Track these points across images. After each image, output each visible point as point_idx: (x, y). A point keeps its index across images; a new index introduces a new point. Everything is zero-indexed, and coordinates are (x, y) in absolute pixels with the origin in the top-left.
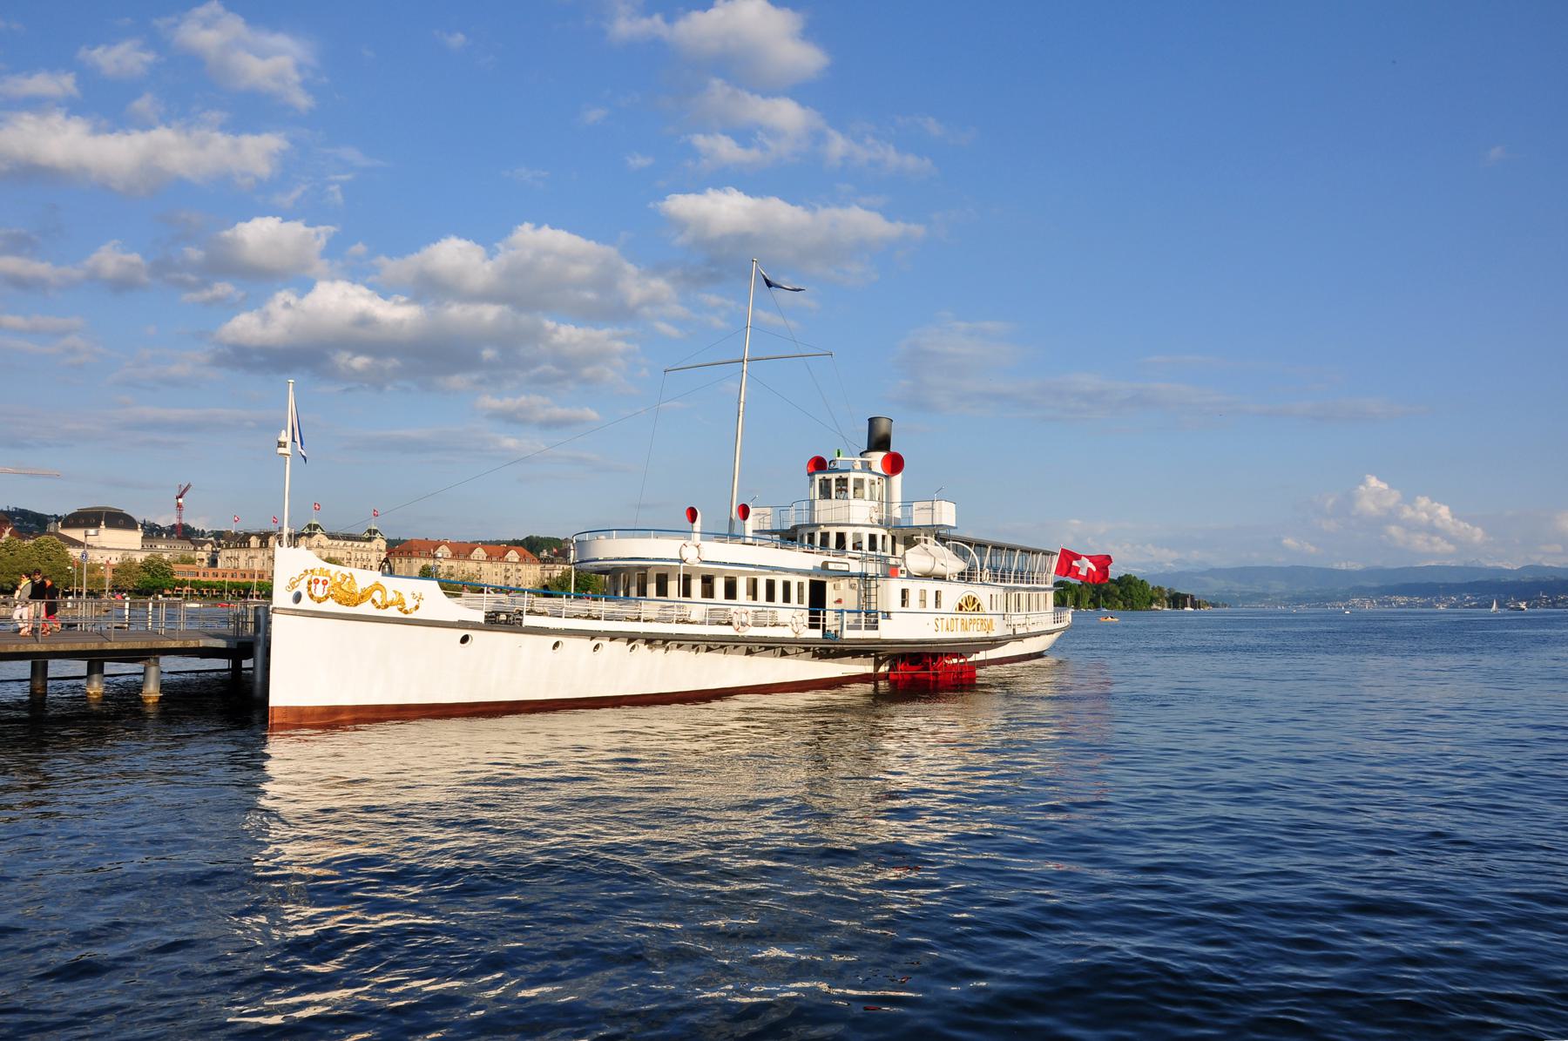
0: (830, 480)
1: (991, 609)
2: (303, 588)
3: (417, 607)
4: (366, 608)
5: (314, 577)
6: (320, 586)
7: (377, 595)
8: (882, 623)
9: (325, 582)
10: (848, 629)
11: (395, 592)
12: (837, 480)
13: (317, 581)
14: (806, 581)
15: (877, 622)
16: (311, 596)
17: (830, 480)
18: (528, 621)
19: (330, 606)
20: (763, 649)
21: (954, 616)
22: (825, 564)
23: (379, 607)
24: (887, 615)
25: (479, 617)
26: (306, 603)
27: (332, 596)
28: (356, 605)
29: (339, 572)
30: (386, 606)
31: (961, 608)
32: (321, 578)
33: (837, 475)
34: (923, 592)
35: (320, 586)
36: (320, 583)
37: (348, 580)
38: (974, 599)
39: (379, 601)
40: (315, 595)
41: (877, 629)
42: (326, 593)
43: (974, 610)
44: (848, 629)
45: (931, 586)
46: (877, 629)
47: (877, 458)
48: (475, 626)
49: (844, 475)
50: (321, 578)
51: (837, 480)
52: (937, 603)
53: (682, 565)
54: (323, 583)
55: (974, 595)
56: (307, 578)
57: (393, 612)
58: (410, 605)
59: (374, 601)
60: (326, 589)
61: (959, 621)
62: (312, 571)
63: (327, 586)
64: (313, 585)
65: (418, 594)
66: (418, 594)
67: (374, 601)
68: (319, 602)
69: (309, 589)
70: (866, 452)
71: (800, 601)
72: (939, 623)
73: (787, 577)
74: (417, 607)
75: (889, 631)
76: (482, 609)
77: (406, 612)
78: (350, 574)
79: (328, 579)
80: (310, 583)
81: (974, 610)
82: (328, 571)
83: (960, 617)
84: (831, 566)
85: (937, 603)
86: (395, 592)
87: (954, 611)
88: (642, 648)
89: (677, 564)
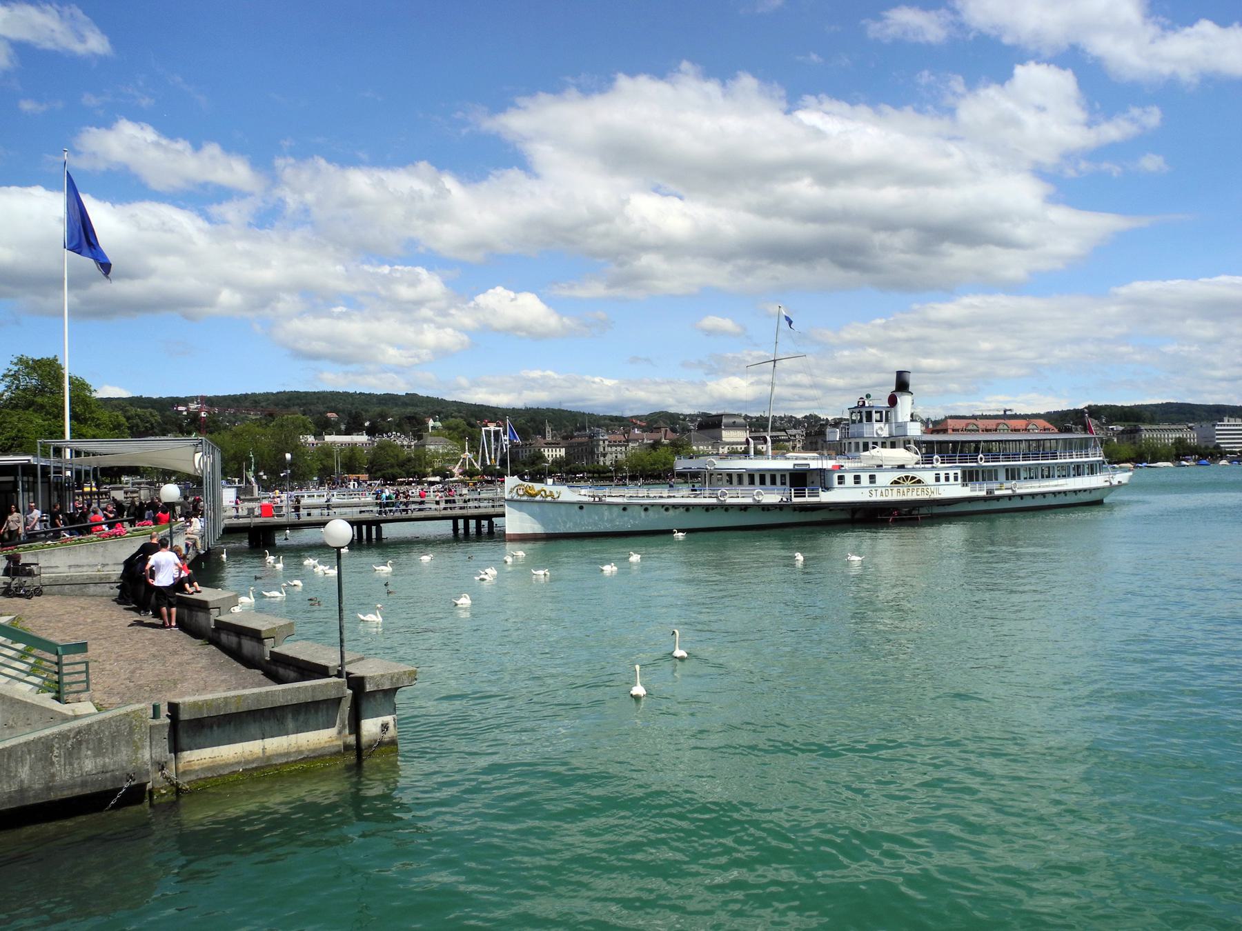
1: (938, 479)
4: (538, 498)
7: (543, 493)
11: (551, 492)
22: (795, 465)
30: (547, 496)
43: (914, 483)
48: (588, 503)
57: (549, 499)
58: (556, 496)
68: (521, 496)
71: (784, 484)
72: (874, 492)
75: (825, 497)
81: (914, 483)
83: (895, 489)
86: (551, 492)
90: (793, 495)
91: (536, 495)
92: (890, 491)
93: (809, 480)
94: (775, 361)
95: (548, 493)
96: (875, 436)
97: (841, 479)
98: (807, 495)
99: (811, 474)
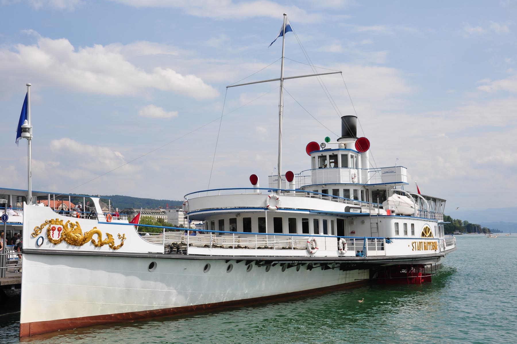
0: (326, 156)
2: (43, 233)
3: (122, 245)
4: (87, 247)
5: (52, 226)
6: (56, 232)
7: (95, 237)
8: (386, 245)
9: (59, 230)
10: (368, 250)
11: (108, 235)
12: (330, 156)
13: (53, 229)
14: (335, 219)
15: (383, 245)
16: (50, 240)
17: (326, 156)
18: (191, 251)
19: (63, 247)
20: (319, 265)
21: (421, 241)
22: (348, 209)
23: (96, 246)
24: (388, 240)
25: (161, 249)
26: (47, 246)
27: (64, 239)
28: (81, 245)
29: (69, 221)
31: (423, 235)
32: (57, 227)
33: (331, 153)
34: (405, 225)
35: (56, 232)
36: (57, 229)
37: (75, 227)
38: (429, 229)
39: (97, 241)
40: (53, 239)
41: (383, 249)
42: (60, 237)
43: (429, 236)
44: (368, 250)
45: (409, 222)
46: (383, 249)
47: (352, 143)
48: (158, 257)
49: (335, 153)
50: (57, 227)
51: (330, 156)
52: (413, 233)
53: (266, 211)
54: (58, 230)
55: (428, 227)
56: (47, 226)
57: (106, 249)
58: (117, 243)
59: (93, 242)
60: (60, 234)
61: (423, 243)
62: (50, 222)
63: (61, 232)
64: (51, 232)
65: (122, 236)
66: (122, 236)
67: (93, 242)
69: (48, 235)
70: (340, 138)
71: (333, 233)
72: (414, 245)
73: (326, 218)
74: (122, 245)
76: (162, 244)
77: (115, 249)
78: (77, 223)
79: (62, 227)
80: (48, 231)
82: (62, 221)
84: (351, 211)
85: (413, 233)
86: (108, 235)
87: (420, 237)
88: (255, 268)
89: (263, 210)
90: (367, 247)
91: (85, 240)
92: (421, 243)
93: (347, 229)
94: (281, 79)
95: (104, 238)
96: (352, 183)
97: (397, 224)
98: (376, 247)
99: (352, 223)
